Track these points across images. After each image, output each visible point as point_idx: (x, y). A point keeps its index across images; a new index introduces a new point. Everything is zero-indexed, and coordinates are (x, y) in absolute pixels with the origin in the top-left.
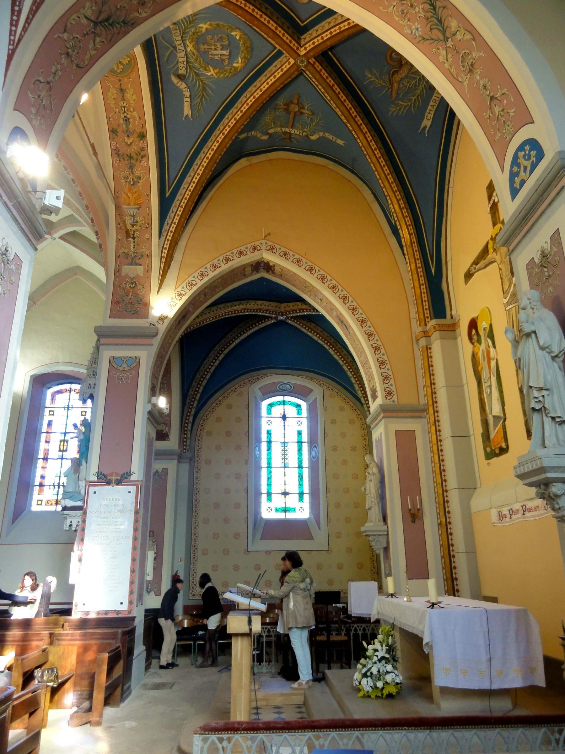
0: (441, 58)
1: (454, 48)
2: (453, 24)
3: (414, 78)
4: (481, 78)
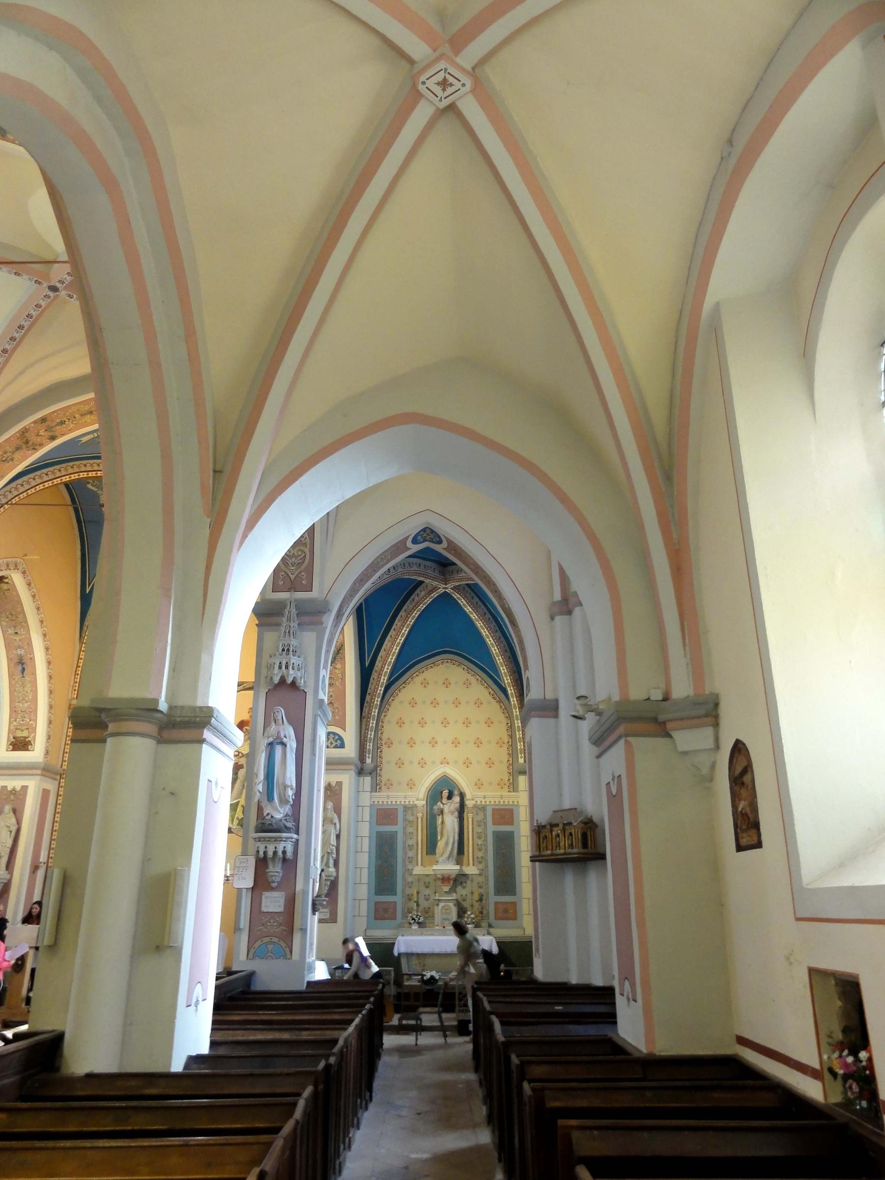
2: (339, 666)
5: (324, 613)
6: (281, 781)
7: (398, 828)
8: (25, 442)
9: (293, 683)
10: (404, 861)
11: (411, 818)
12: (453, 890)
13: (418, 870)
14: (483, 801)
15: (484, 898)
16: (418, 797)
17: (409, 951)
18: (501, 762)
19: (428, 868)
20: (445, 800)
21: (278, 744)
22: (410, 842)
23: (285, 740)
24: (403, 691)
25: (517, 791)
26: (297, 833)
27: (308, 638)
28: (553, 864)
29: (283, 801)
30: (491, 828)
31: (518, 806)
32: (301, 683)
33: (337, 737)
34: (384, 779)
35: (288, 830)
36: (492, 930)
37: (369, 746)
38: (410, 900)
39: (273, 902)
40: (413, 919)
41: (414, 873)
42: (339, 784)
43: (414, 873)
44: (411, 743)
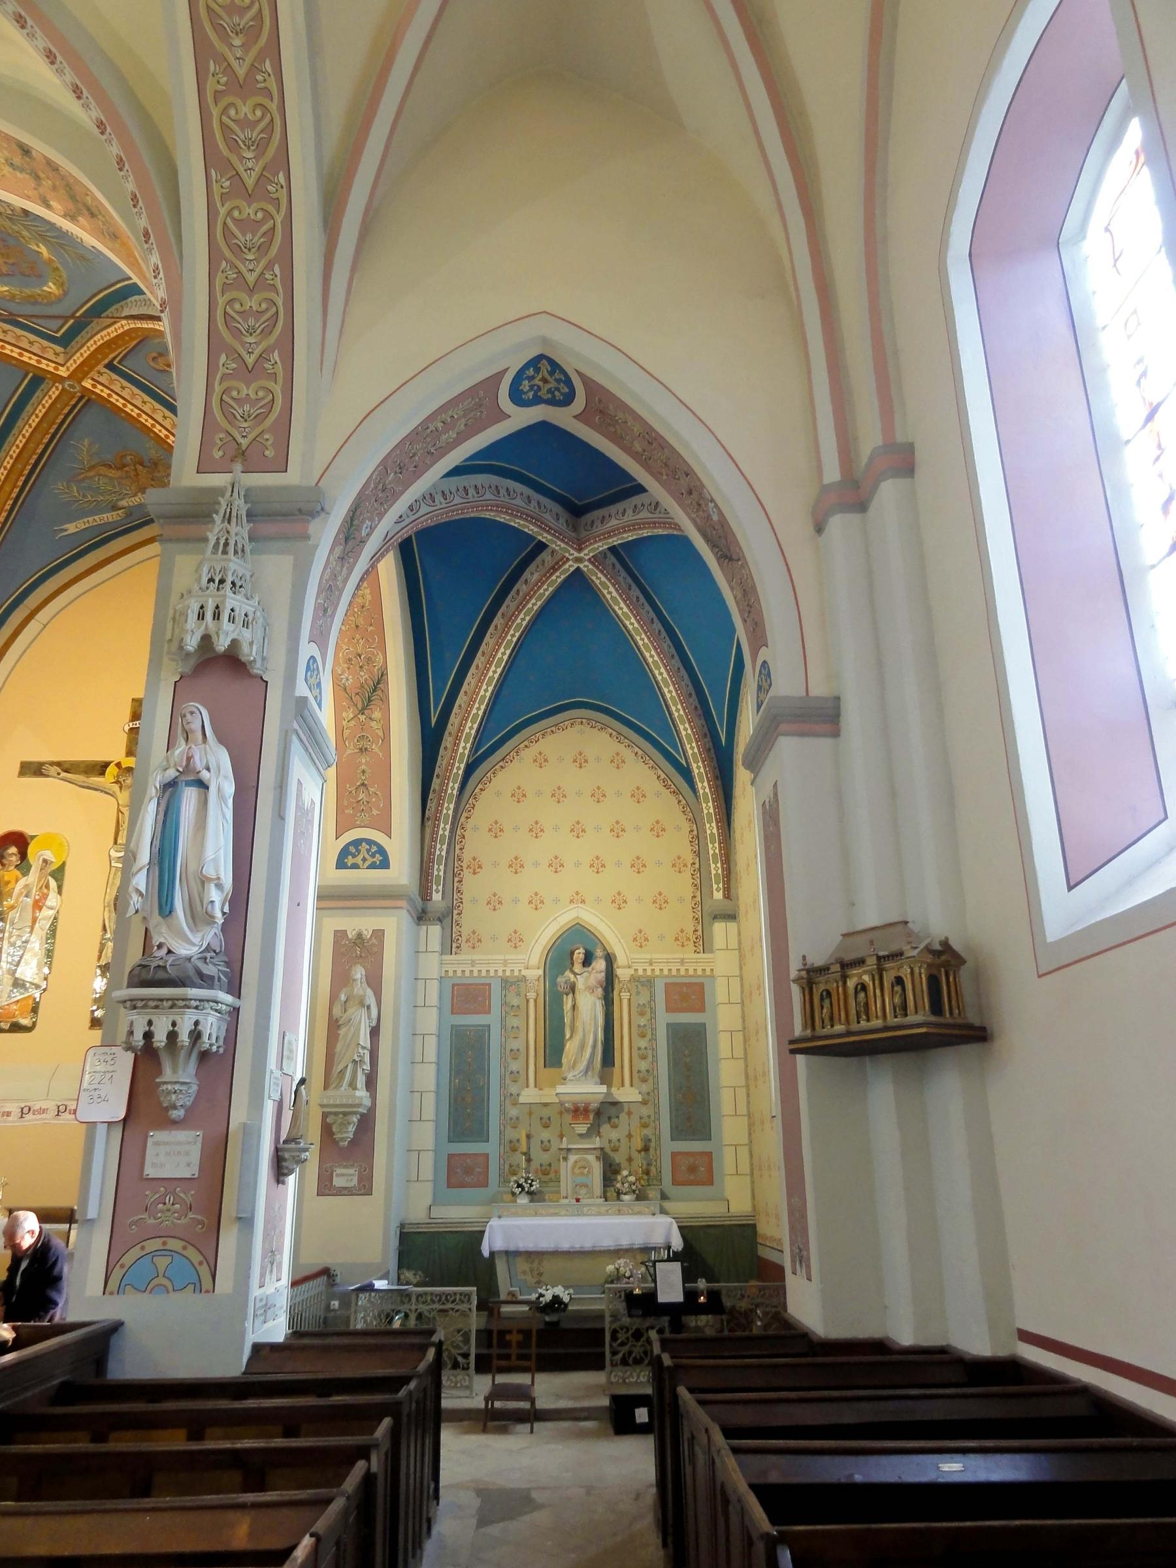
0: (344, 714)
1: (362, 724)
2: (377, 715)
3: (114, 487)
4: (367, 763)
5: (313, 517)
6: (192, 868)
7: (492, 1019)
10: (502, 1078)
11: (515, 1001)
12: (595, 1130)
13: (529, 1095)
14: (649, 969)
15: (653, 1144)
16: (529, 962)
17: (512, 1248)
18: (681, 900)
19: (547, 1091)
20: (578, 968)
21: (188, 784)
22: (514, 1045)
23: (205, 775)
24: (500, 774)
25: (712, 952)
26: (235, 988)
27: (275, 567)
28: (842, 1061)
29: (199, 916)
30: (664, 1018)
31: (712, 977)
32: (249, 653)
33: (374, 849)
34: (466, 930)
35: (206, 981)
36: (667, 1205)
37: (439, 870)
38: (514, 1150)
39: (173, 1155)
40: (519, 1186)
41: (521, 1100)
42: (379, 934)
43: (521, 1100)
44: (516, 865)
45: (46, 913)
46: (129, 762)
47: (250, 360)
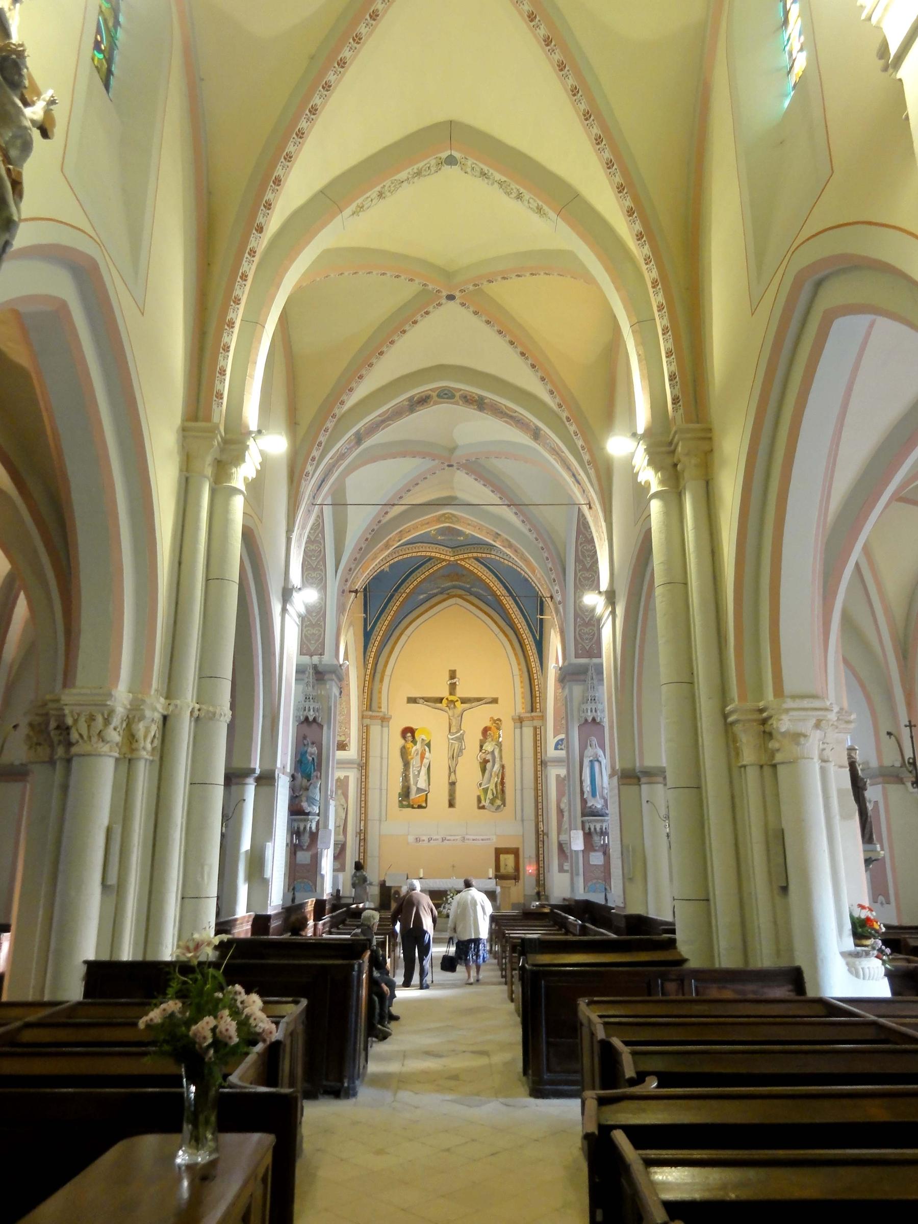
8: (387, 546)
9: (594, 720)
45: (426, 761)
46: (452, 698)
47: (587, 620)
